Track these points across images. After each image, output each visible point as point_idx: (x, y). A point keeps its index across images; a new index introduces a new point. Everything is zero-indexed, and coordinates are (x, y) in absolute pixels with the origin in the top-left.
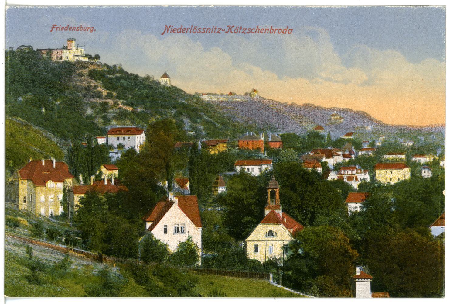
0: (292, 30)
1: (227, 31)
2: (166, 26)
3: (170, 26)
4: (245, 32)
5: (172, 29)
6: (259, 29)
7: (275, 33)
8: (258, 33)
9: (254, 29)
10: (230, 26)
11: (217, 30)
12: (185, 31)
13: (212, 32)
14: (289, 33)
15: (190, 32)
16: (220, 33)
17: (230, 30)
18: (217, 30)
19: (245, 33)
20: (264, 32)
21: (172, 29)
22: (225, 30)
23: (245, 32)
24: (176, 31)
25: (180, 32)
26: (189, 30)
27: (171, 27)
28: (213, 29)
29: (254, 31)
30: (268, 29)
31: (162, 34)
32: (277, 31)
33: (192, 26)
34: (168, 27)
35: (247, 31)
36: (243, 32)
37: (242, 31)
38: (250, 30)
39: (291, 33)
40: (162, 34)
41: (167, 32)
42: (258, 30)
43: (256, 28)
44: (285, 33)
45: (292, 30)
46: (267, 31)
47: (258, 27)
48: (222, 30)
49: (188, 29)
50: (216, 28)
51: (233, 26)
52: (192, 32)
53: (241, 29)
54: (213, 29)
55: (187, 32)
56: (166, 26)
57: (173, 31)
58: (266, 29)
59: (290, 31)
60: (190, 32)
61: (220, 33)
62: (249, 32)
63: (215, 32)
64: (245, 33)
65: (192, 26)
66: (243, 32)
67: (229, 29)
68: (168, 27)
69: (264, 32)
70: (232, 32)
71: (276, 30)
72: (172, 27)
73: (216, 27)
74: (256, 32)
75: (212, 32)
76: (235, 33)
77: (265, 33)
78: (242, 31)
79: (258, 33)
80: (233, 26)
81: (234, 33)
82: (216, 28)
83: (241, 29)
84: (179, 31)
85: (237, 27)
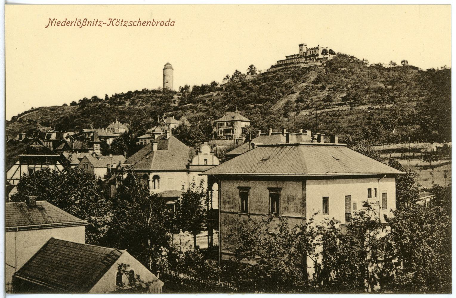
0: (174, 22)
1: (109, 24)
2: (50, 19)
3: (54, 19)
4: (127, 25)
5: (56, 22)
6: (141, 22)
7: (157, 25)
8: (140, 25)
9: (136, 22)
10: (112, 19)
11: (98, 23)
12: (70, 24)
13: (93, 25)
14: (171, 25)
15: (75, 25)
16: (101, 26)
17: (112, 23)
18: (98, 23)
19: (126, 26)
20: (146, 24)
21: (56, 22)
22: (106, 23)
23: (127, 25)
24: (60, 24)
25: (64, 25)
26: (73, 24)
27: (55, 21)
28: (94, 22)
29: (135, 24)
30: (150, 22)
31: (46, 27)
32: (159, 24)
33: (76, 19)
34: (52, 20)
35: (129, 24)
36: (124, 25)
37: (123, 23)
38: (132, 23)
39: (173, 25)
40: (46, 27)
41: (51, 26)
42: (140, 23)
43: (138, 21)
44: (168, 25)
45: (174, 22)
46: (149, 23)
47: (139, 19)
48: (104, 23)
49: (72, 22)
50: (97, 22)
51: (115, 19)
52: (76, 24)
53: (122, 22)
54: (94, 22)
55: (71, 25)
56: (50, 19)
57: (57, 24)
58: (148, 22)
59: (172, 24)
60: (75, 25)
61: (101, 26)
62: (131, 25)
63: (96, 25)
64: (126, 26)
65: (76, 19)
66: (124, 25)
67: (111, 22)
68: (52, 20)
69: (146, 24)
70: (113, 25)
71: (158, 22)
72: (56, 20)
73: (97, 20)
74: (137, 25)
75: (93, 25)
76: (117, 25)
77: (147, 25)
78: (123, 23)
79: (140, 25)
80: (115, 19)
81: (115, 25)
82: (97, 22)
83: (122, 22)
84: (63, 24)
85: (118, 20)
